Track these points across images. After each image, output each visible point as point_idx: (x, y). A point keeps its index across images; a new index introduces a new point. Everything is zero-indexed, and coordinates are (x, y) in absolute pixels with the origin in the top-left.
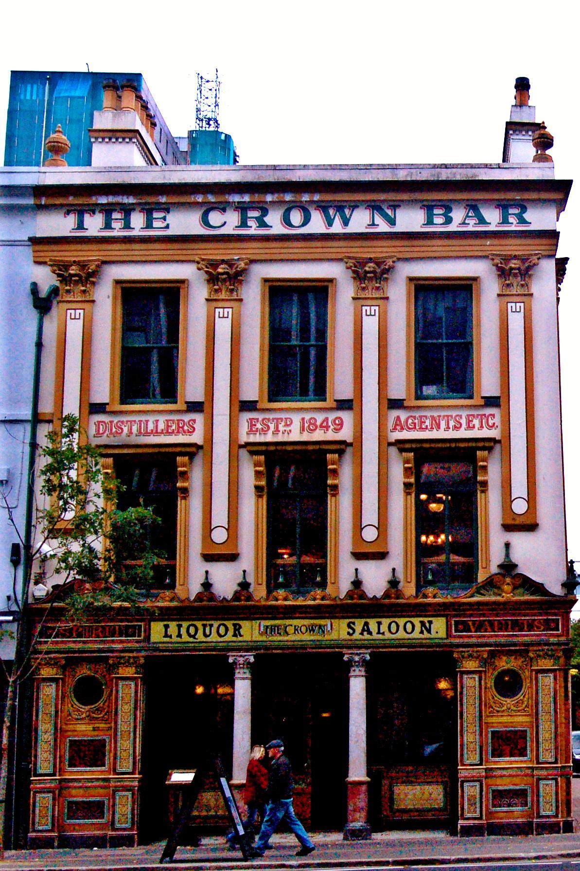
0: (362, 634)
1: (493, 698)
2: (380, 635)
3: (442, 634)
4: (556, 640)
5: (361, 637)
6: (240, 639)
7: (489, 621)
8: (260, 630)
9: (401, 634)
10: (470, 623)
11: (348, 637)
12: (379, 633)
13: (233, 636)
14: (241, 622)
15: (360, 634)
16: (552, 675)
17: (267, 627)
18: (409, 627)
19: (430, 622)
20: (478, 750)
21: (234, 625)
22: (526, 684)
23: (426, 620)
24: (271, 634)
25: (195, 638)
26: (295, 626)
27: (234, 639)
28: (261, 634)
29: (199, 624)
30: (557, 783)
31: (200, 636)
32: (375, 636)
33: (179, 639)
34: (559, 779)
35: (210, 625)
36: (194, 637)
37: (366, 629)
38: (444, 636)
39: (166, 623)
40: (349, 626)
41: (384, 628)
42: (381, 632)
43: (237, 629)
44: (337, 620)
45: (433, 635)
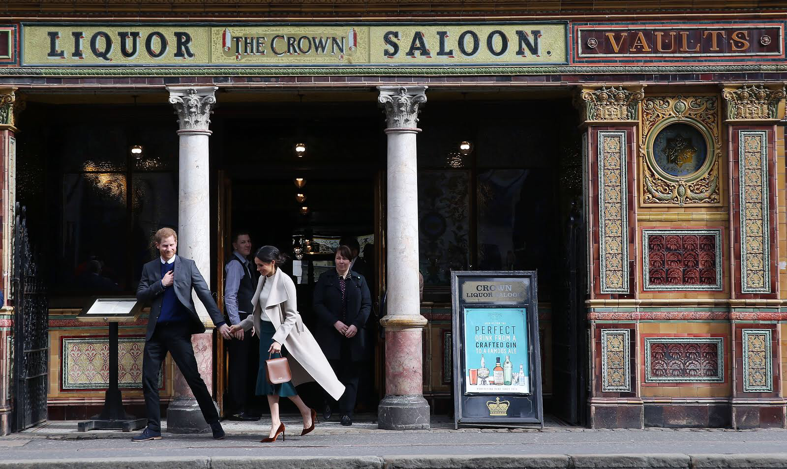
0: (411, 53)
1: (653, 175)
2: (445, 57)
3: (558, 56)
4: (774, 67)
5: (409, 60)
6: (188, 61)
7: (644, 31)
8: (224, 44)
9: (483, 56)
10: (611, 36)
11: (386, 60)
12: (442, 52)
13: (176, 55)
14: (189, 30)
15: (408, 54)
16: (764, 134)
17: (238, 39)
18: (497, 43)
19: (536, 34)
20: (626, 269)
21: (178, 35)
22: (714, 149)
23: (528, 29)
24: (246, 52)
25: (107, 59)
26: (289, 39)
27: (179, 60)
28: (228, 53)
29: (113, 32)
30: (774, 333)
31: (116, 56)
32: (435, 59)
33: (76, 60)
34: (779, 326)
35: (132, 34)
36: (104, 55)
37: (418, 46)
38: (562, 60)
39: (53, 29)
40: (387, 39)
41: (451, 44)
42: (447, 50)
43: (183, 42)
44: (365, 29)
45: (542, 58)
